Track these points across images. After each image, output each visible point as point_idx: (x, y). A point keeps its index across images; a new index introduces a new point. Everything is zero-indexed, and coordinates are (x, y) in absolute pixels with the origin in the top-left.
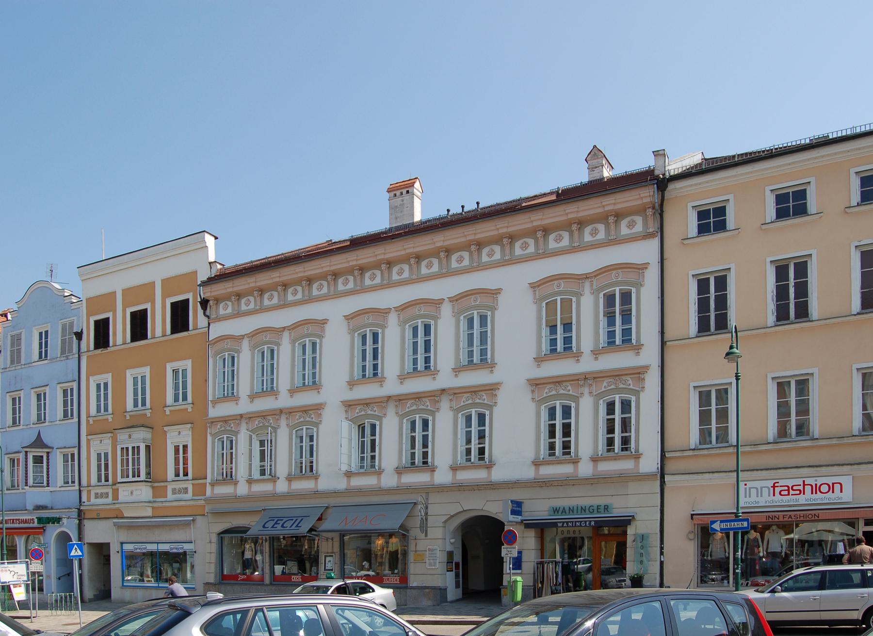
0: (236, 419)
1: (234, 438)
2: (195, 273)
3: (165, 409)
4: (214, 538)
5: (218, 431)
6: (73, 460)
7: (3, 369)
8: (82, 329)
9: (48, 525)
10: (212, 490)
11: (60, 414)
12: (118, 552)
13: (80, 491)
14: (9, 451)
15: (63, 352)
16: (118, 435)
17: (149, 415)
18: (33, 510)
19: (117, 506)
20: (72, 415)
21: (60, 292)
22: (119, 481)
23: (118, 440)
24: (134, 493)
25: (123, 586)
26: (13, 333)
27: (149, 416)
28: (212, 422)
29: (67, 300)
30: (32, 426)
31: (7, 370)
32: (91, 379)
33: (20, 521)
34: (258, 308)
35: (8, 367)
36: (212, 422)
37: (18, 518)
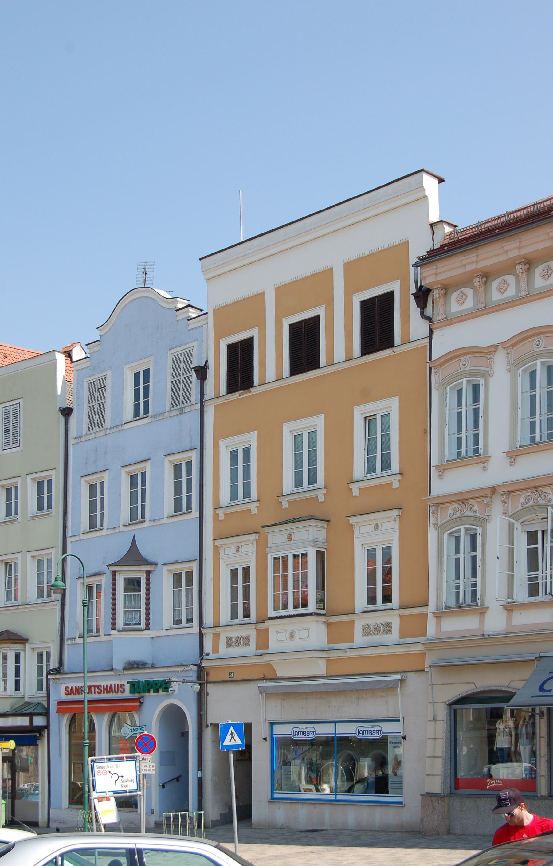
0: (483, 496)
1: (479, 531)
2: (404, 246)
3: (352, 486)
4: (442, 713)
5: (448, 518)
6: (189, 582)
8: (207, 362)
9: (147, 694)
10: (439, 625)
11: (169, 506)
12: (265, 739)
13: (201, 635)
15: (174, 402)
16: (269, 536)
17: (321, 498)
18: (124, 670)
19: (266, 659)
20: (189, 507)
21: (169, 303)
22: (270, 615)
23: (270, 545)
24: (297, 635)
25: (272, 798)
26: (92, 378)
27: (323, 500)
28: (438, 504)
29: (181, 315)
30: (122, 529)
31: (83, 439)
32: (222, 444)
34: (523, 293)
35: (84, 435)
36: (438, 504)
37: (97, 684)
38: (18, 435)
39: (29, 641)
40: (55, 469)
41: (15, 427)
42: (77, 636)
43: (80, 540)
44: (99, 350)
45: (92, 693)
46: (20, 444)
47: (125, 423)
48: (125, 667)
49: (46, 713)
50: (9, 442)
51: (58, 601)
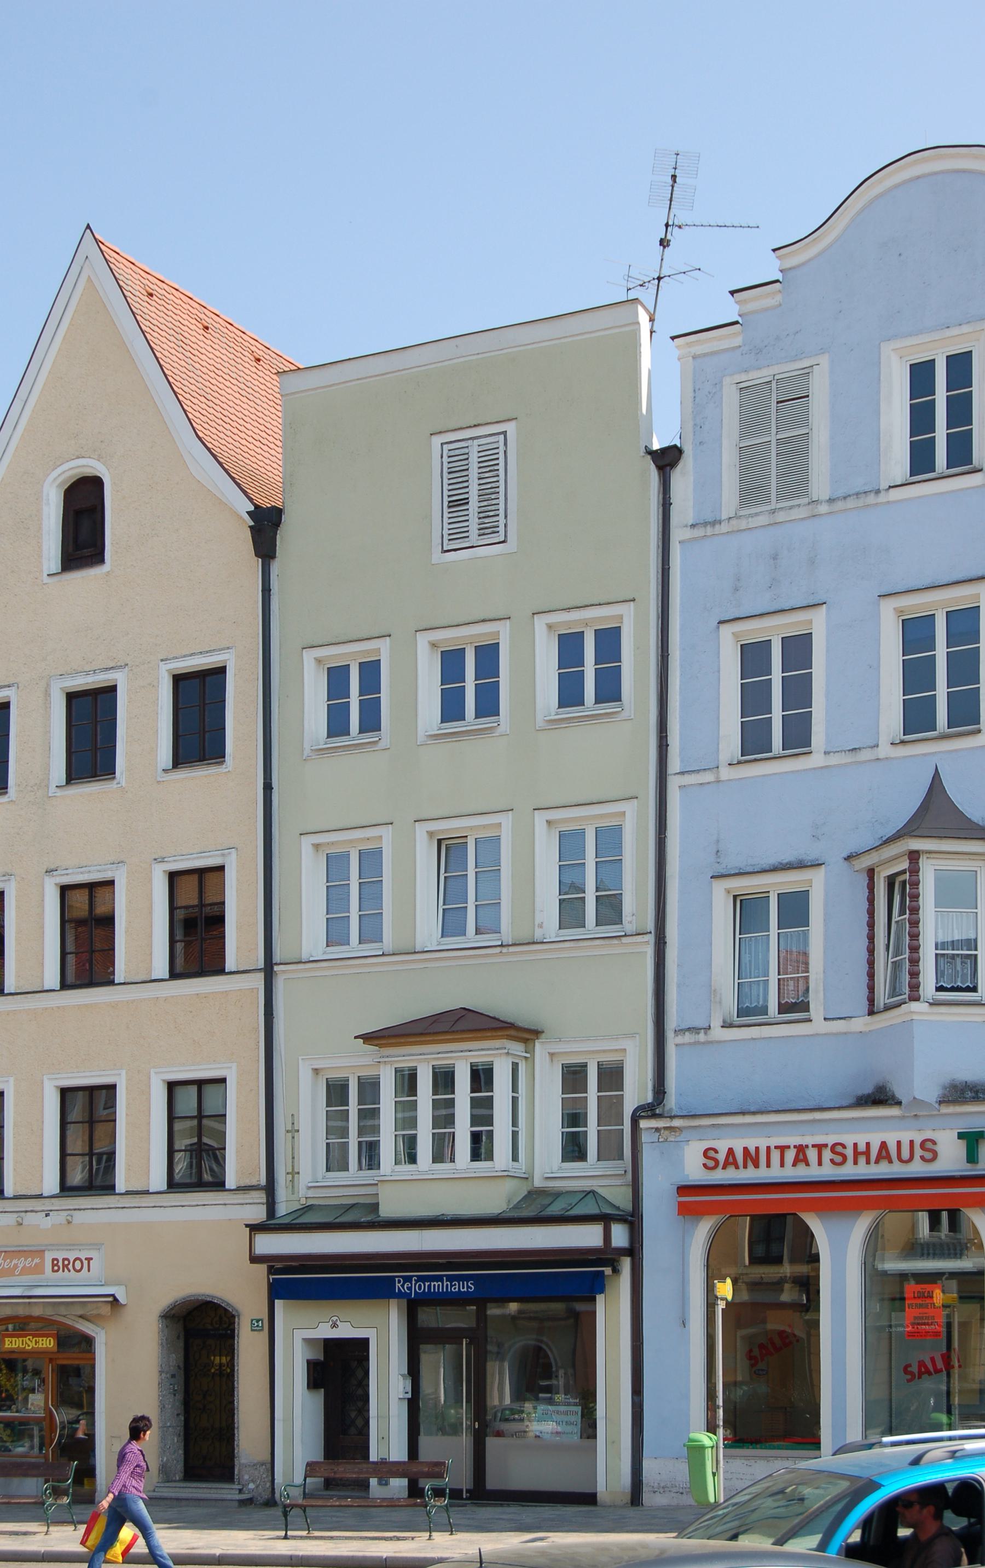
7: (693, 526)
14: (733, 861)
18: (940, 1103)
26: (753, 374)
31: (724, 528)
33: (849, 1152)
35: (724, 516)
37: (830, 1140)
38: (502, 512)
39: (543, 1035)
40: (633, 600)
41: (487, 494)
42: (716, 1023)
43: (719, 781)
44: (780, 305)
45: (807, 1164)
46: (506, 536)
47: (890, 487)
48: (944, 1096)
49: (633, 1220)
50: (468, 531)
51: (650, 933)
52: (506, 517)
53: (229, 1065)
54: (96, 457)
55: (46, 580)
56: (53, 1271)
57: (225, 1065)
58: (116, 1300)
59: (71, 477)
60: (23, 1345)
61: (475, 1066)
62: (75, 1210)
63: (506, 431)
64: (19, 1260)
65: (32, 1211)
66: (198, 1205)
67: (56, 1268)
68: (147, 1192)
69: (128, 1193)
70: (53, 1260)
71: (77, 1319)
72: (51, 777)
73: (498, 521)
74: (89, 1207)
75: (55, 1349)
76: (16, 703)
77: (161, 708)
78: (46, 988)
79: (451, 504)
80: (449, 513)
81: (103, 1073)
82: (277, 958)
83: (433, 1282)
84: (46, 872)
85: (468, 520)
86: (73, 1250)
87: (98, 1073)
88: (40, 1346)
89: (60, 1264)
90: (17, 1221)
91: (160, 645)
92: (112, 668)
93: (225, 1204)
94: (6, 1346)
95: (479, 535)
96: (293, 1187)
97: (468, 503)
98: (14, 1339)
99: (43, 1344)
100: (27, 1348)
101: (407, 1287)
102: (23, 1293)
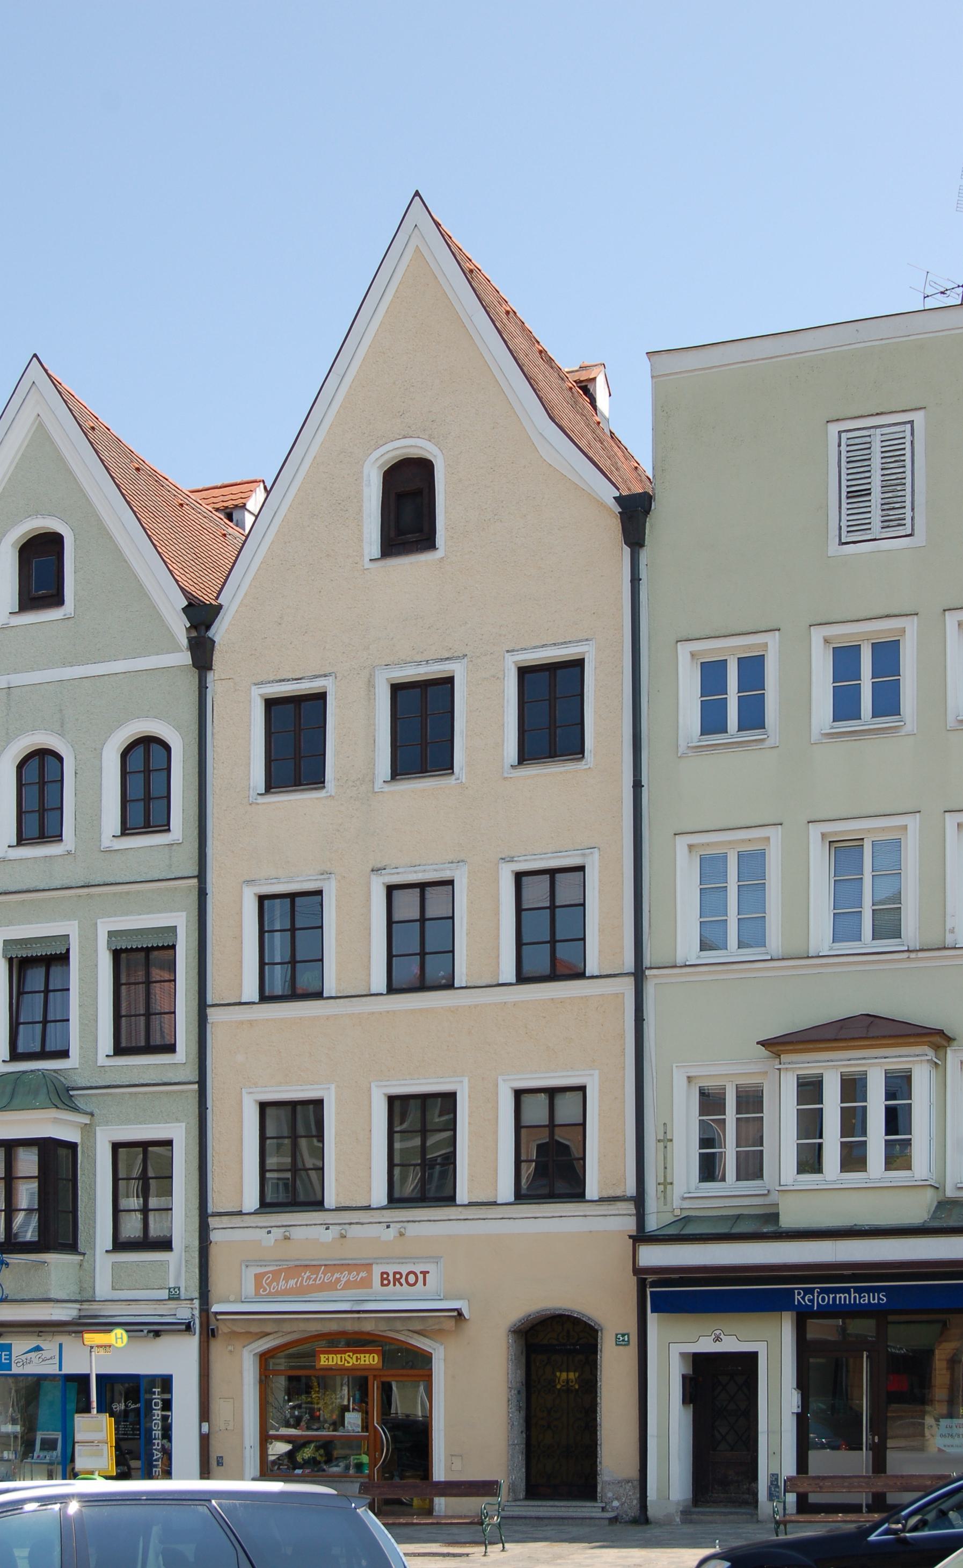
39: (955, 1043)
41: (893, 485)
46: (913, 529)
50: (870, 523)
52: (913, 509)
53: (591, 1072)
54: (426, 437)
55: (368, 565)
56: (382, 1285)
57: (587, 1072)
58: (460, 1314)
59: (393, 458)
60: (341, 1361)
61: (889, 1073)
62: (408, 1221)
63: (913, 421)
64: (342, 1274)
65: (357, 1223)
66: (553, 1217)
67: (385, 1282)
68: (495, 1204)
69: (471, 1204)
70: (382, 1273)
71: (410, 1334)
72: (376, 772)
73: (905, 514)
74: (426, 1219)
75: (380, 1366)
76: (334, 693)
77: (508, 701)
78: (372, 992)
79: (850, 495)
80: (848, 503)
81: (442, 1080)
82: (647, 962)
83: (839, 1294)
84: (373, 871)
85: (870, 512)
86: (406, 1263)
87: (436, 1080)
88: (362, 1362)
89: (391, 1278)
90: (341, 1234)
91: (505, 635)
92: (447, 659)
93: (585, 1216)
94: (322, 1363)
95: (882, 528)
96: (665, 1198)
97: (870, 494)
98: (331, 1356)
99: (365, 1361)
100: (346, 1364)
101: (808, 1300)
102: (352, 1308)
